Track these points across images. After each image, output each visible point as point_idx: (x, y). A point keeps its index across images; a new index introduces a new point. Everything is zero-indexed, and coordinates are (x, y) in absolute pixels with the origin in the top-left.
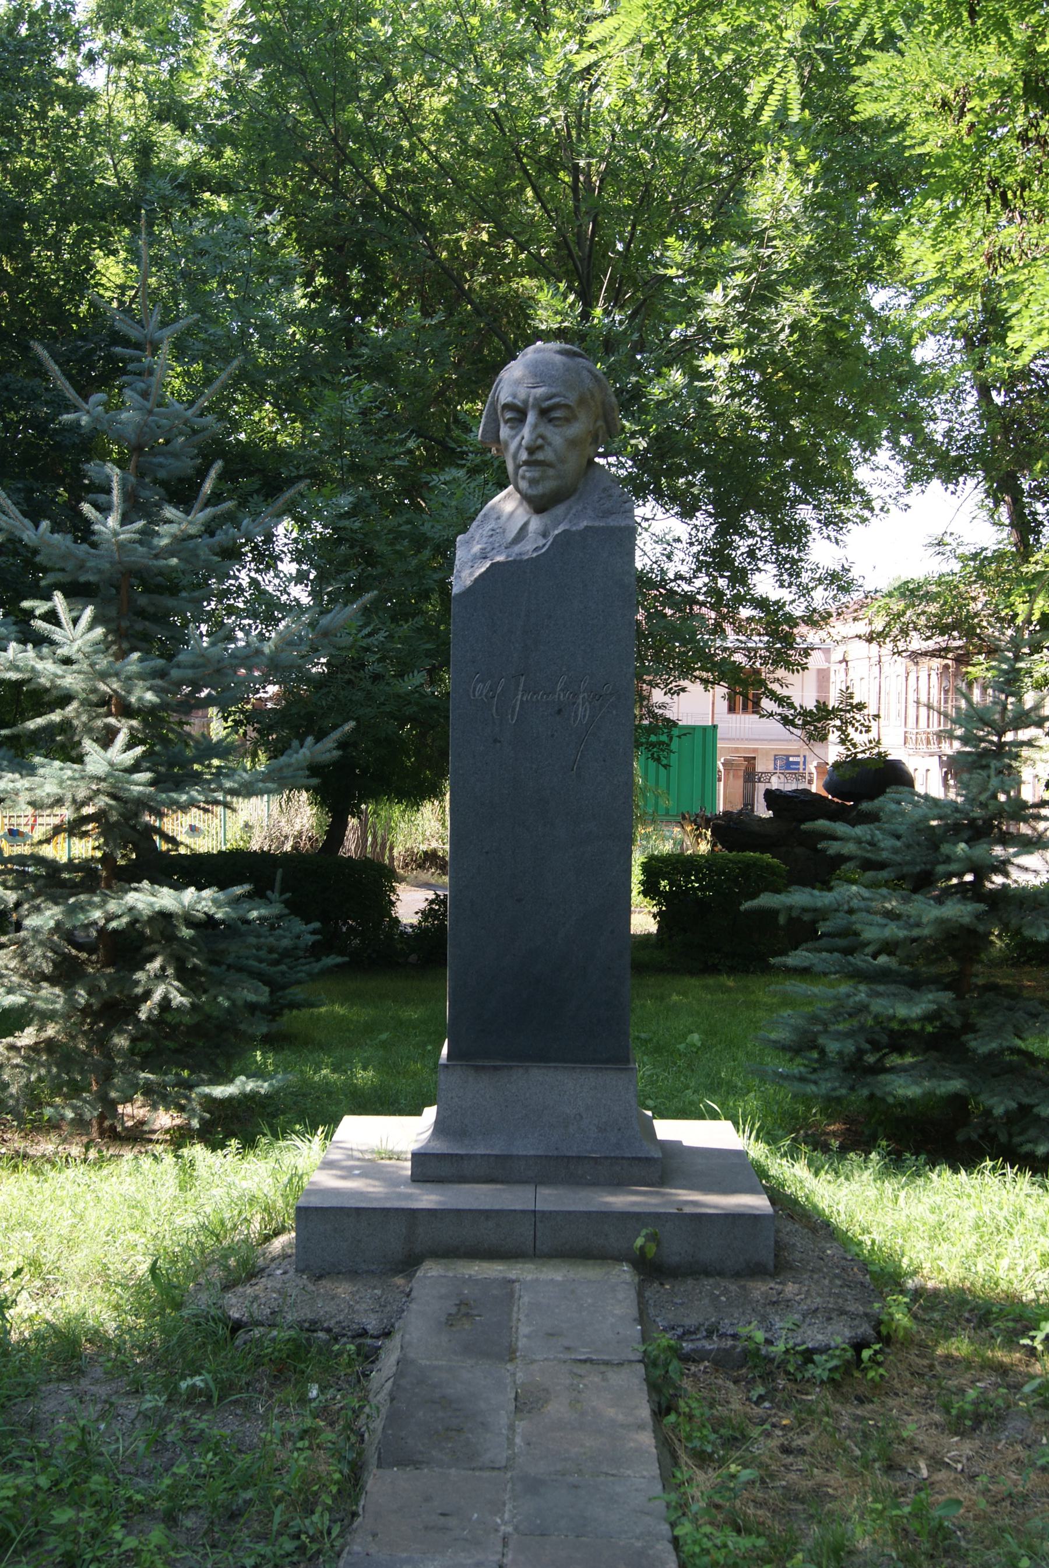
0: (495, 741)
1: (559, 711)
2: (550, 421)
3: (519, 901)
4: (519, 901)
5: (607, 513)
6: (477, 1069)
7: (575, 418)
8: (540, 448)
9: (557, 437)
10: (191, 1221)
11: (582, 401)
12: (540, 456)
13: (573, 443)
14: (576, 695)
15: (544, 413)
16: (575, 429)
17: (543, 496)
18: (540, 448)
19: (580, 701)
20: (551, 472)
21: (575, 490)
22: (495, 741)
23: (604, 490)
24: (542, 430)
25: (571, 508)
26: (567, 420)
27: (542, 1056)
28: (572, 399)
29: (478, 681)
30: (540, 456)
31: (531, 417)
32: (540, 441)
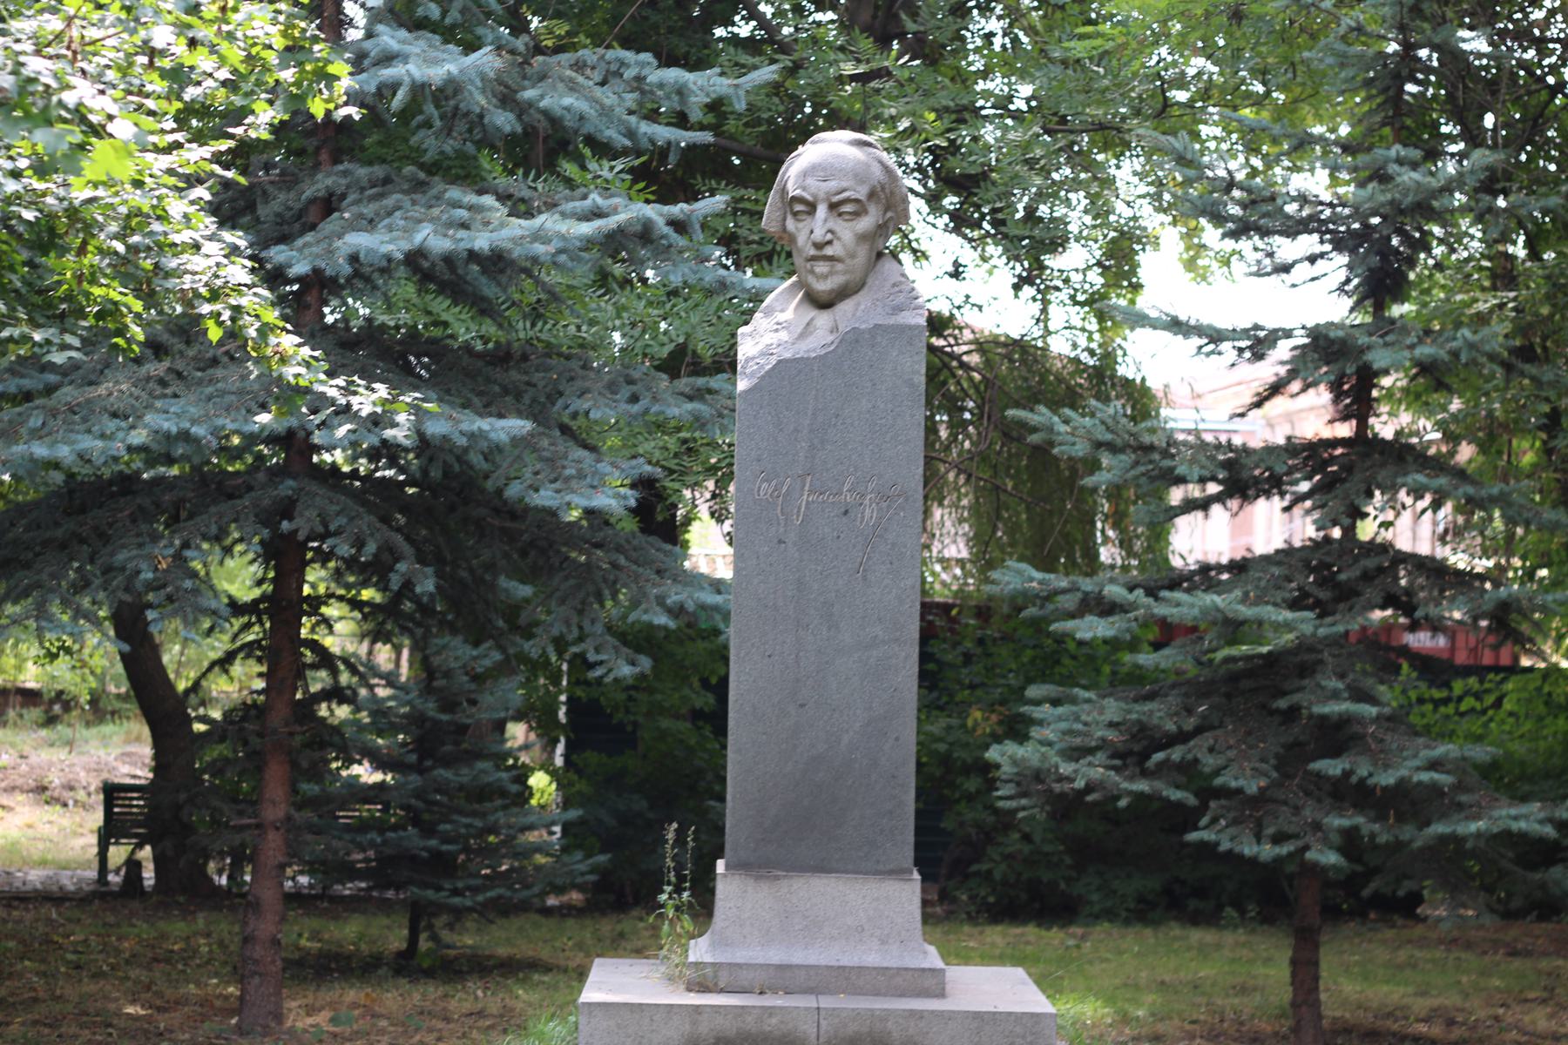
0: (780, 542)
1: (846, 512)
2: (840, 215)
3: (802, 706)
4: (802, 706)
5: (899, 309)
6: (758, 878)
7: (866, 212)
8: (830, 243)
9: (847, 231)
10: (530, 953)
11: (872, 195)
12: (829, 251)
13: (862, 238)
15: (833, 207)
16: (866, 223)
17: (832, 291)
18: (830, 243)
19: (867, 502)
20: (839, 267)
21: (863, 284)
22: (780, 542)
23: (894, 285)
25: (859, 304)
26: (856, 214)
27: (821, 868)
28: (861, 193)
29: (763, 480)
30: (829, 251)
31: (822, 211)
32: (829, 236)
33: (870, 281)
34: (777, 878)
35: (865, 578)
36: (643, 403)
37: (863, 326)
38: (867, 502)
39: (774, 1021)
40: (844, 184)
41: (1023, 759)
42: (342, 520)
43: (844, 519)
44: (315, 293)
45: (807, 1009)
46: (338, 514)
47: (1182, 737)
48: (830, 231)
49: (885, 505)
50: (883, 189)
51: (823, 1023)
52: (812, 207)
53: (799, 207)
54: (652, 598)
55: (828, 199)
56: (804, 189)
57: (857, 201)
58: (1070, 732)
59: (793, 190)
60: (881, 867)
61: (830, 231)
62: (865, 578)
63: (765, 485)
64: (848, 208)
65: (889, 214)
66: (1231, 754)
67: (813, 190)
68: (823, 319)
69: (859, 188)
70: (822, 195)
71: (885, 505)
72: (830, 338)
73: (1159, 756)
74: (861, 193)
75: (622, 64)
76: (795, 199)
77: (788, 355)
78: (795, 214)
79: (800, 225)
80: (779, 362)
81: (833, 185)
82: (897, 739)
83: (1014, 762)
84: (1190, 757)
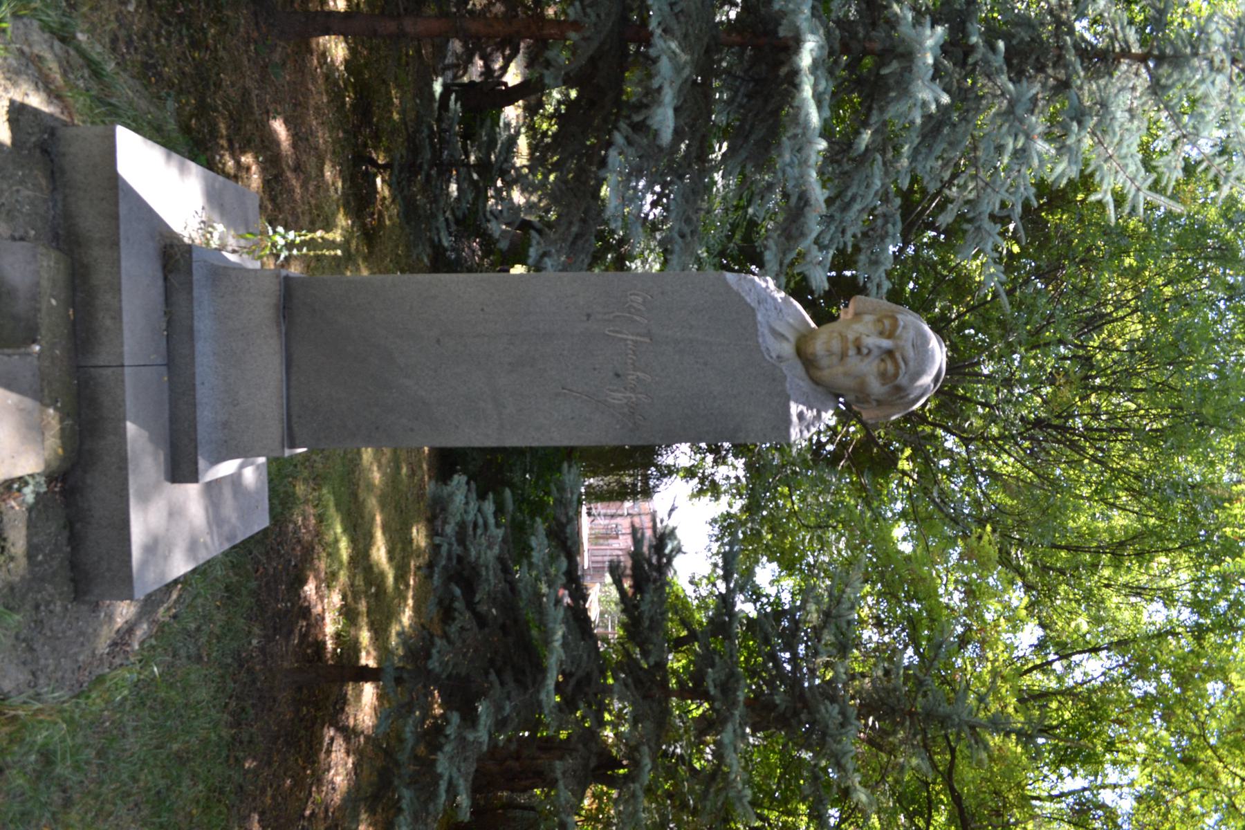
0: (589, 316)
1: (617, 375)
3: (438, 341)
14: (633, 390)
15: (890, 353)
19: (628, 394)
22: (589, 316)
24: (876, 352)
26: (883, 375)
29: (645, 299)
32: (865, 351)
33: (820, 389)
34: (278, 325)
35: (558, 395)
36: (680, 240)
37: (788, 385)
38: (628, 394)
39: (108, 322)
40: (911, 364)
41: (452, 501)
42: (594, 18)
43: (611, 374)
44: (738, 39)
45: (121, 355)
46: (598, 16)
47: (470, 605)
48: (870, 352)
49: (626, 410)
50: (902, 398)
51: (109, 371)
52: (891, 335)
53: (887, 322)
54: (548, 249)
55: (897, 347)
56: (904, 327)
57: (896, 375)
58: (475, 526)
59: (899, 317)
60: (295, 419)
61: (870, 352)
62: (558, 395)
63: (640, 300)
64: (890, 367)
65: (874, 403)
66: (459, 644)
67: (905, 335)
68: (787, 349)
69: (907, 377)
70: (901, 343)
71: (626, 410)
72: (774, 355)
73: (458, 591)
74: (902, 380)
75: (894, 225)
76: (896, 320)
77: (759, 317)
78: (879, 320)
79: (870, 326)
80: (753, 310)
81: (911, 353)
82: (412, 430)
83: (451, 495)
84: (456, 614)
